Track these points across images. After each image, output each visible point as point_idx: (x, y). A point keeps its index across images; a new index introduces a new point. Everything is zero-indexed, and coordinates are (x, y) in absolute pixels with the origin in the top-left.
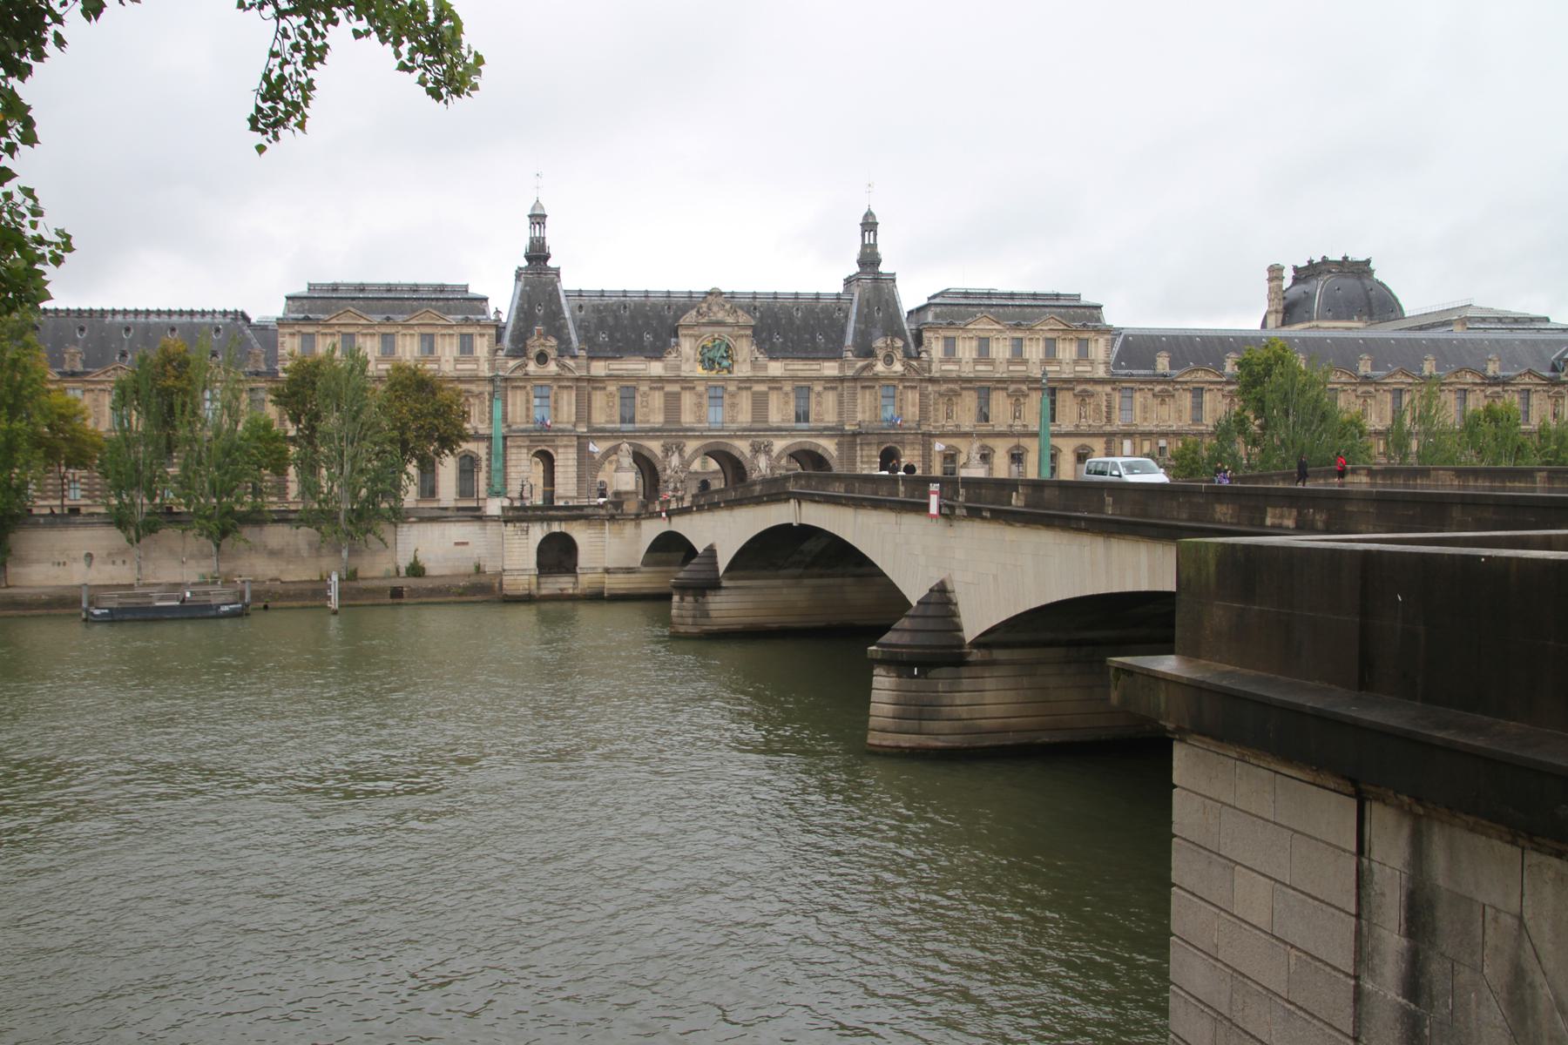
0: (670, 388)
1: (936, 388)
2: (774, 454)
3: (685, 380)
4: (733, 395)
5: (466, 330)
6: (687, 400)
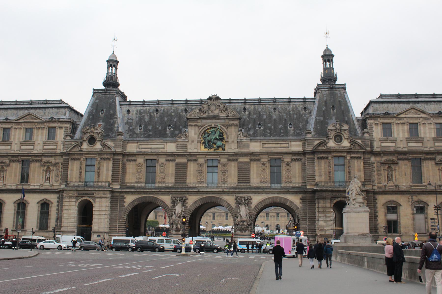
1: (378, 159)
2: (253, 206)
3: (190, 154)
4: (224, 165)
5: (52, 125)
6: (192, 168)
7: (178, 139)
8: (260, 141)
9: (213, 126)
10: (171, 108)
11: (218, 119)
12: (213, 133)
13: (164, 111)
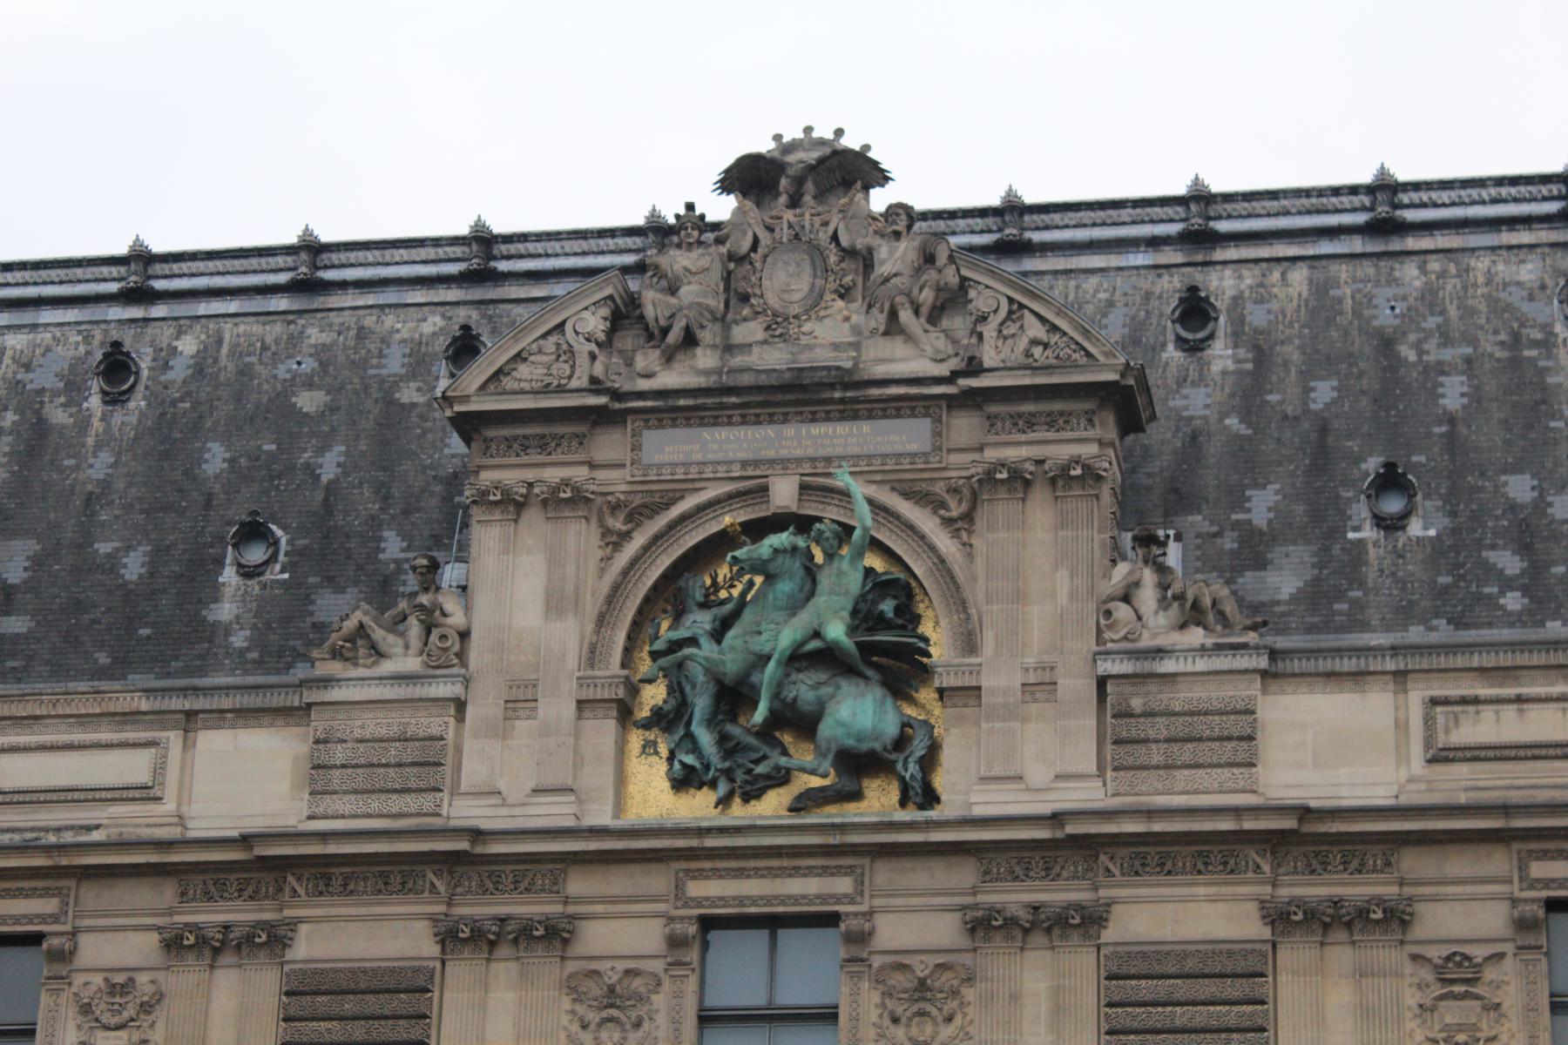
0: (335, 936)
3: (467, 861)
7: (334, 668)
8: (1400, 676)
9: (784, 494)
10: (294, 340)
11: (851, 411)
12: (785, 587)
13: (200, 368)
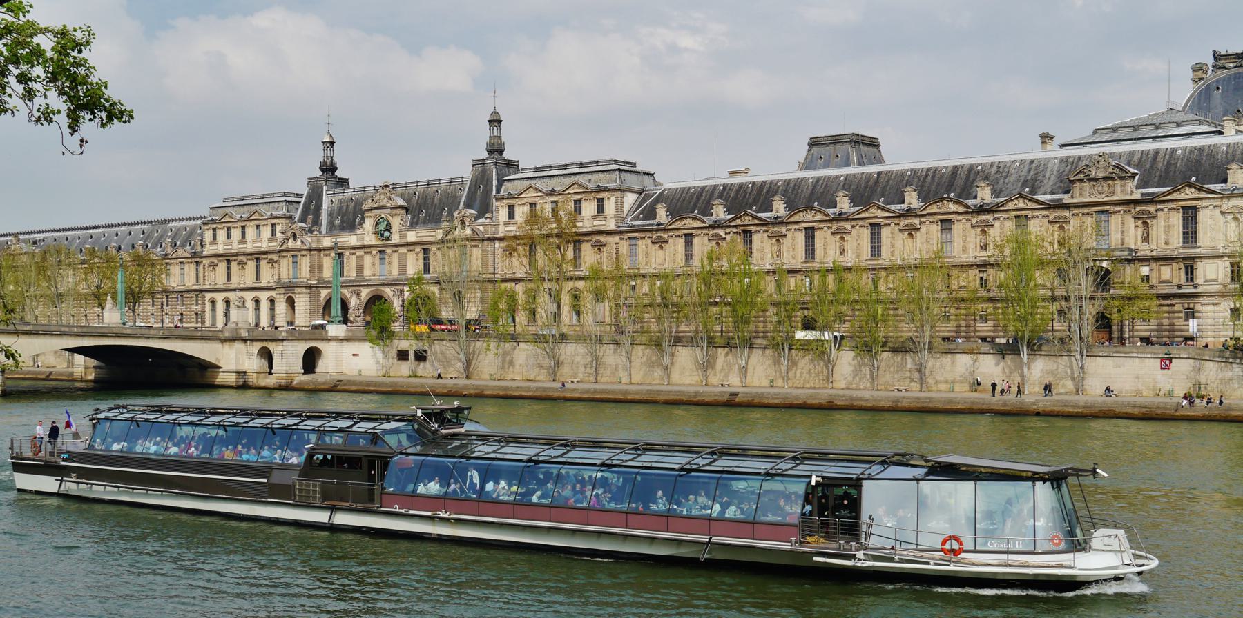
1: (503, 244)
4: (390, 256)
6: (368, 260)
